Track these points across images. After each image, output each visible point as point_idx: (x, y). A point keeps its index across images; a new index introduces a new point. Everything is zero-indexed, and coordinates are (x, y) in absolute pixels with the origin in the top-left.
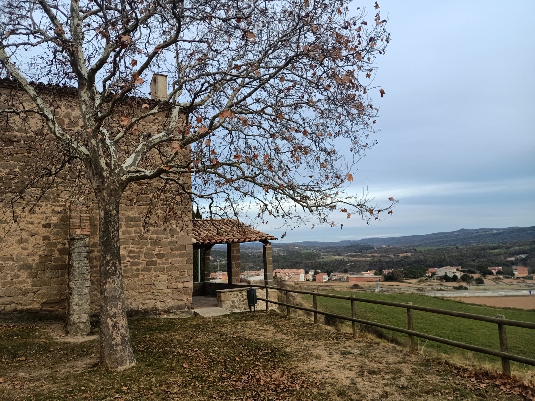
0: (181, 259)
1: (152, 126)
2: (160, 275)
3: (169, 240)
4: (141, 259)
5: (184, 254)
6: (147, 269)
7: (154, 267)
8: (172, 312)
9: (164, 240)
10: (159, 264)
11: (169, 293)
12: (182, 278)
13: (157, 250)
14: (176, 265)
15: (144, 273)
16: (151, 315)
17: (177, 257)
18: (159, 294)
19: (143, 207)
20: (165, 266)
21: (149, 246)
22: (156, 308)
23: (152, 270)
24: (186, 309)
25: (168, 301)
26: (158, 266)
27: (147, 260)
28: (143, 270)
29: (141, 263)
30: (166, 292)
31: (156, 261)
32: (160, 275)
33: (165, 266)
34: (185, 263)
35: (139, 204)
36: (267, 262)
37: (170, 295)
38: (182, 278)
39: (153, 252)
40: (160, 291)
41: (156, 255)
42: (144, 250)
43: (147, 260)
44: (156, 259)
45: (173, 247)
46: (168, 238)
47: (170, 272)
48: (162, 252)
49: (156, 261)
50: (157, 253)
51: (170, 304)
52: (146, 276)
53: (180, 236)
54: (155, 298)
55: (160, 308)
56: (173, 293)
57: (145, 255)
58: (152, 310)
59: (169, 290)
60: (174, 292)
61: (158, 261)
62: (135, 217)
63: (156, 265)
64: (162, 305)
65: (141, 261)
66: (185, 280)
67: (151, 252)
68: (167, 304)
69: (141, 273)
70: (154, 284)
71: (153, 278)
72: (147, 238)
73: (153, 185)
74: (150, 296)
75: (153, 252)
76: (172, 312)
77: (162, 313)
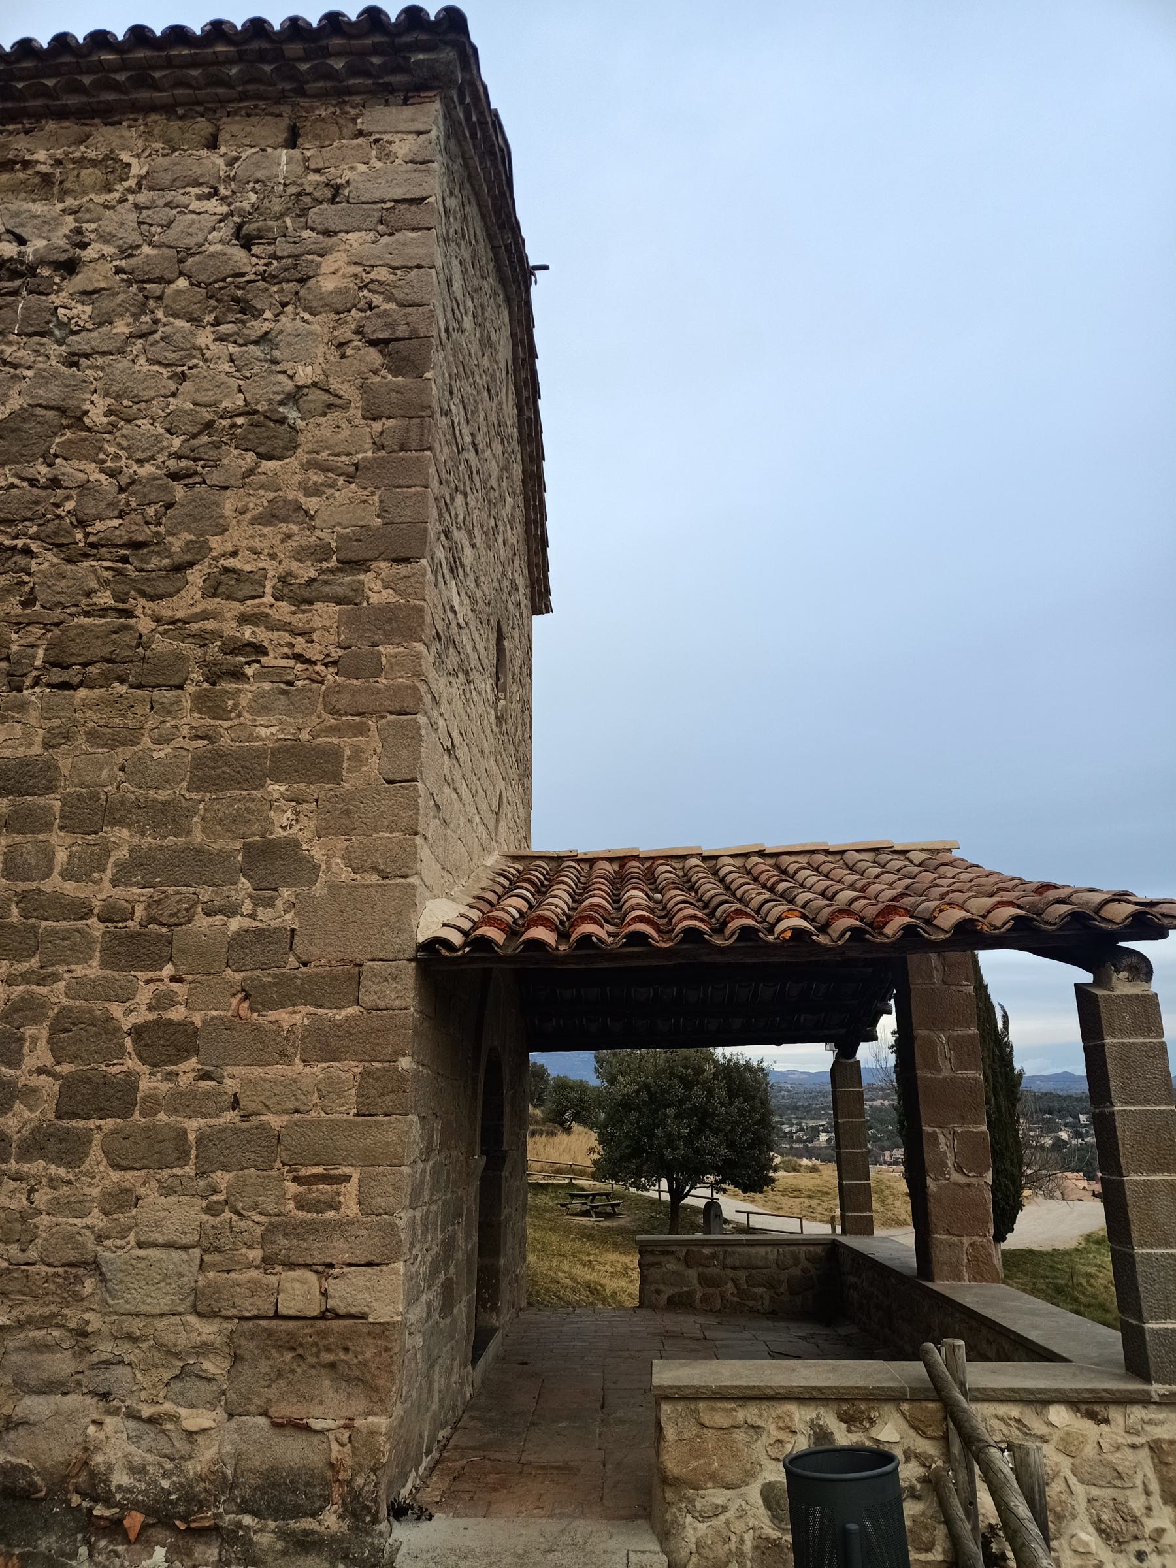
0: (317, 1068)
1: (195, 205)
2: (150, 1194)
3: (235, 924)
4: (30, 1062)
5: (345, 1029)
6: (64, 1137)
7: (109, 1123)
8: (216, 1529)
9: (202, 922)
10: (153, 1104)
11: (203, 1349)
12: (313, 1228)
13: (144, 995)
14: (276, 1122)
15: (37, 1166)
16: (47, 1528)
17: (284, 1057)
18: (131, 1353)
19: (82, 693)
20: (193, 1126)
21: (92, 970)
22: (93, 1474)
23: (96, 1152)
24: (331, 1521)
25: (194, 1420)
26: (138, 1118)
27: (65, 1069)
28: (33, 1146)
29: (29, 1094)
30: (182, 1340)
31: (130, 1083)
32: (150, 1194)
33: (193, 1126)
34: (346, 1108)
35: (57, 676)
36: (1124, 1135)
37: (209, 1366)
38: (313, 1228)
39: (116, 1010)
40: (136, 1326)
41: (137, 1032)
42: (56, 994)
43: (65, 1069)
44: (132, 1063)
45: (265, 977)
46: (231, 910)
47: (222, 1179)
48: (177, 1014)
49: (130, 1083)
50: (144, 1015)
51: (206, 1455)
52: (42, 1197)
53: (319, 890)
54: (98, 1380)
55: (120, 1478)
56: (236, 1358)
57: (55, 1030)
58: (60, 1482)
59: (207, 1330)
60: (248, 1347)
61: (145, 1085)
62: (24, 762)
63: (125, 1113)
64: (139, 1454)
65: (23, 1076)
66: (340, 1250)
67: (98, 1007)
68: (181, 1445)
69: (13, 1165)
70: (94, 1266)
71: (95, 1218)
72: (82, 911)
73: (165, 552)
74: (61, 1364)
75: (116, 1010)
76: (213, 1531)
77: (134, 1521)
